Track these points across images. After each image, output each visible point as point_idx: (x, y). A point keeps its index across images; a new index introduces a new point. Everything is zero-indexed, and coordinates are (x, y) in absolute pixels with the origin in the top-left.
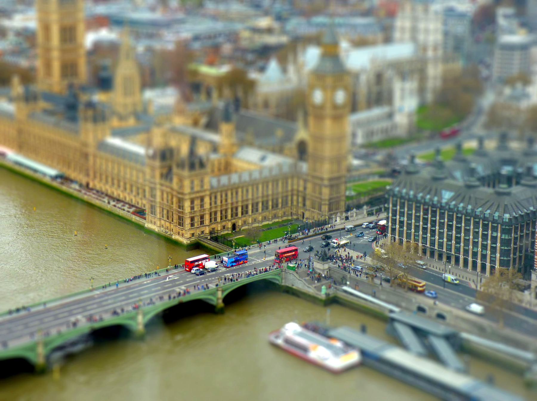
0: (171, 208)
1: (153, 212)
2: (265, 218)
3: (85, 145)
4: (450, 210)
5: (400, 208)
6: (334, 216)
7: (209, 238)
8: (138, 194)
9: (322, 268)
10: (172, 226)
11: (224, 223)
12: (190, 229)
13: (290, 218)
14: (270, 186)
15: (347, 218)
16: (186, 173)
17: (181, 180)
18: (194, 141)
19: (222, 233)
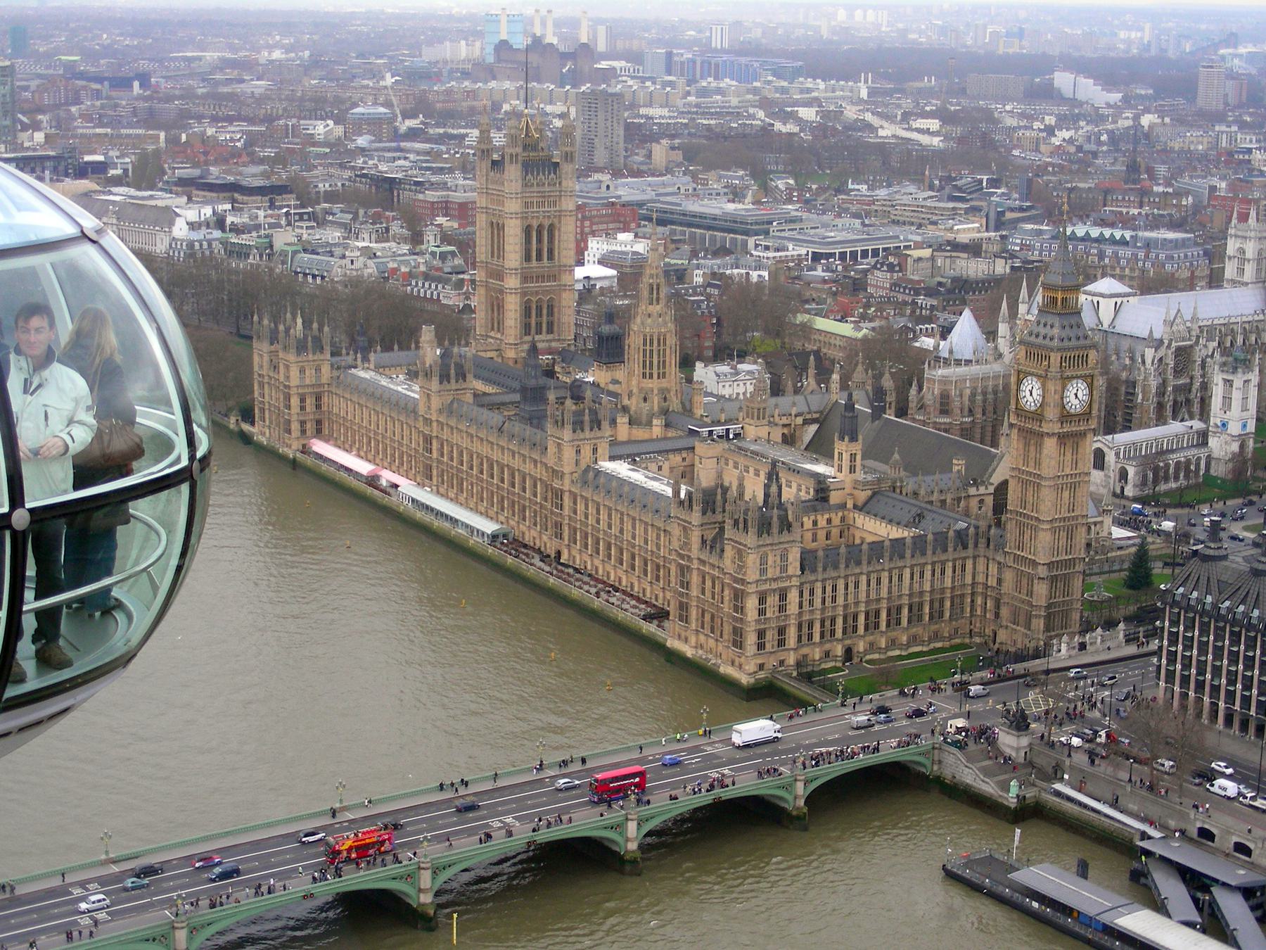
0: (719, 609)
1: (685, 618)
2: (914, 640)
3: (561, 476)
5: (1185, 630)
6: (1055, 641)
7: (795, 674)
8: (658, 579)
9: (1015, 746)
10: (720, 648)
11: (827, 646)
12: (755, 655)
13: (967, 641)
14: (928, 574)
15: (1083, 646)
16: (750, 539)
17: (740, 554)
18: (773, 476)
19: (823, 666)
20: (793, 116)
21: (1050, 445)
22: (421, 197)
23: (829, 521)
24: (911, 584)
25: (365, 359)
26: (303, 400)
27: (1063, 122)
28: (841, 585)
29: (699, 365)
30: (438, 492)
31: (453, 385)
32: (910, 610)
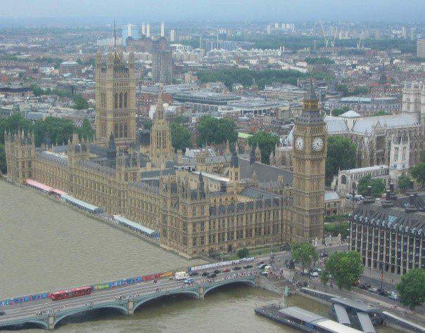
1: (165, 235)
2: (257, 242)
4: (393, 230)
15: (324, 243)
16: (188, 201)
20: (248, 63)
21: (308, 163)
22: (84, 92)
23: (227, 199)
24: (256, 220)
25: (50, 147)
26: (23, 163)
27: (361, 63)
28: (226, 220)
29: (187, 149)
30: (75, 197)
31: (81, 154)
32: (256, 231)
